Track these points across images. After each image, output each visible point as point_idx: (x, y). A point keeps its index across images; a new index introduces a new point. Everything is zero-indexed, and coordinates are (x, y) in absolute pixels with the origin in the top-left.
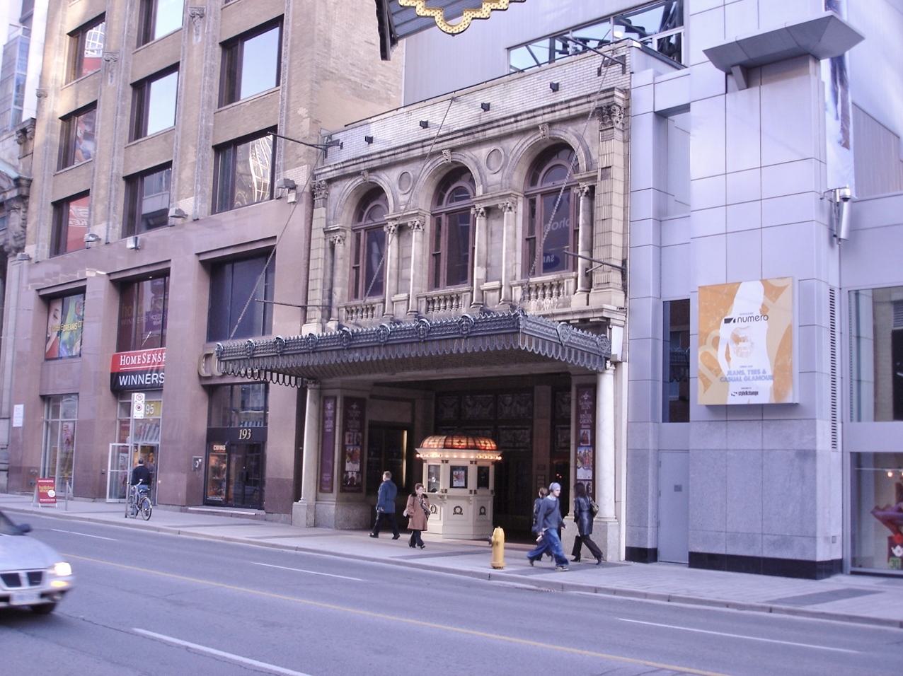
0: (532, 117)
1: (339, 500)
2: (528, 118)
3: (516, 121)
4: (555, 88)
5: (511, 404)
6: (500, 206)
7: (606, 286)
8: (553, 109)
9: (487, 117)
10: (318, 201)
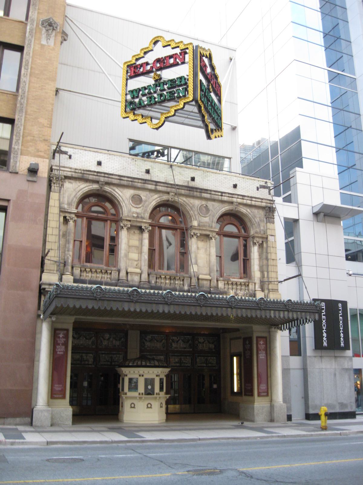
0: (230, 197)
1: (71, 403)
2: (229, 197)
3: (222, 196)
4: (99, 163)
5: (109, 339)
6: (211, 236)
7: (277, 291)
8: (243, 198)
9: (192, 184)
10: (54, 187)
